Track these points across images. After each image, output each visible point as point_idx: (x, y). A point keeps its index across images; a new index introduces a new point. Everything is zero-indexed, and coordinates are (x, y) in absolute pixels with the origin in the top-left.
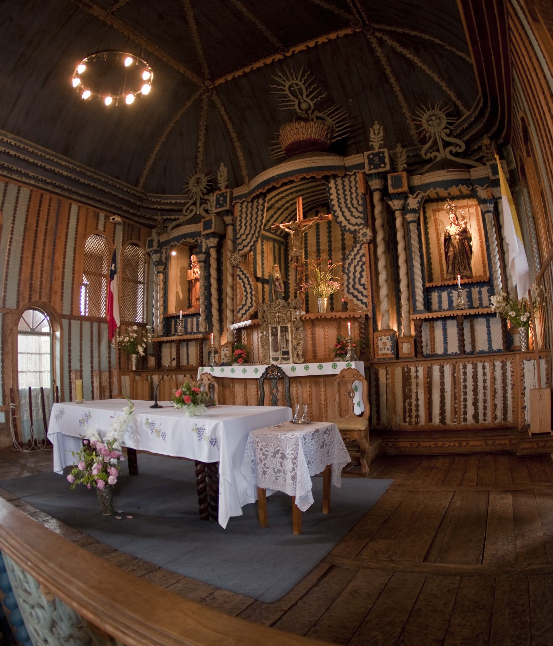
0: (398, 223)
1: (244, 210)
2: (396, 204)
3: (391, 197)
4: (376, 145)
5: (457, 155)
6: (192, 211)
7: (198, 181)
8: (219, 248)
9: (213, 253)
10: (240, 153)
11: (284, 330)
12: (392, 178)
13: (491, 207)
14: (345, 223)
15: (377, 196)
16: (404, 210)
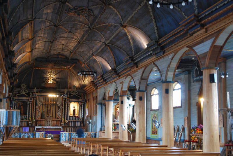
0: (66, 106)
1: (39, 98)
2: (67, 103)
3: (66, 102)
4: (65, 93)
5: (77, 94)
6: (22, 92)
7: (24, 86)
8: (32, 104)
9: (31, 104)
10: (32, 80)
11: (50, 121)
12: (67, 99)
13: (81, 106)
14: (58, 105)
15: (64, 101)
16: (68, 105)
